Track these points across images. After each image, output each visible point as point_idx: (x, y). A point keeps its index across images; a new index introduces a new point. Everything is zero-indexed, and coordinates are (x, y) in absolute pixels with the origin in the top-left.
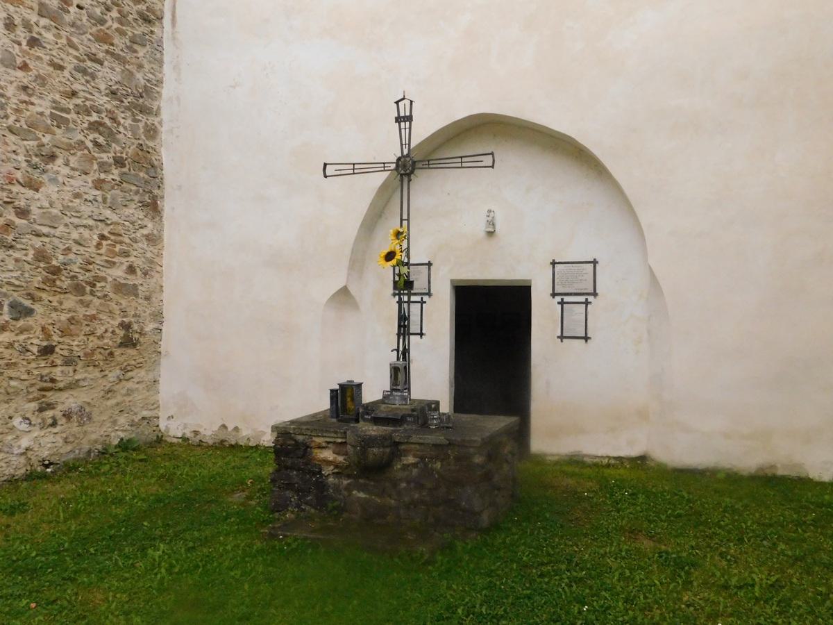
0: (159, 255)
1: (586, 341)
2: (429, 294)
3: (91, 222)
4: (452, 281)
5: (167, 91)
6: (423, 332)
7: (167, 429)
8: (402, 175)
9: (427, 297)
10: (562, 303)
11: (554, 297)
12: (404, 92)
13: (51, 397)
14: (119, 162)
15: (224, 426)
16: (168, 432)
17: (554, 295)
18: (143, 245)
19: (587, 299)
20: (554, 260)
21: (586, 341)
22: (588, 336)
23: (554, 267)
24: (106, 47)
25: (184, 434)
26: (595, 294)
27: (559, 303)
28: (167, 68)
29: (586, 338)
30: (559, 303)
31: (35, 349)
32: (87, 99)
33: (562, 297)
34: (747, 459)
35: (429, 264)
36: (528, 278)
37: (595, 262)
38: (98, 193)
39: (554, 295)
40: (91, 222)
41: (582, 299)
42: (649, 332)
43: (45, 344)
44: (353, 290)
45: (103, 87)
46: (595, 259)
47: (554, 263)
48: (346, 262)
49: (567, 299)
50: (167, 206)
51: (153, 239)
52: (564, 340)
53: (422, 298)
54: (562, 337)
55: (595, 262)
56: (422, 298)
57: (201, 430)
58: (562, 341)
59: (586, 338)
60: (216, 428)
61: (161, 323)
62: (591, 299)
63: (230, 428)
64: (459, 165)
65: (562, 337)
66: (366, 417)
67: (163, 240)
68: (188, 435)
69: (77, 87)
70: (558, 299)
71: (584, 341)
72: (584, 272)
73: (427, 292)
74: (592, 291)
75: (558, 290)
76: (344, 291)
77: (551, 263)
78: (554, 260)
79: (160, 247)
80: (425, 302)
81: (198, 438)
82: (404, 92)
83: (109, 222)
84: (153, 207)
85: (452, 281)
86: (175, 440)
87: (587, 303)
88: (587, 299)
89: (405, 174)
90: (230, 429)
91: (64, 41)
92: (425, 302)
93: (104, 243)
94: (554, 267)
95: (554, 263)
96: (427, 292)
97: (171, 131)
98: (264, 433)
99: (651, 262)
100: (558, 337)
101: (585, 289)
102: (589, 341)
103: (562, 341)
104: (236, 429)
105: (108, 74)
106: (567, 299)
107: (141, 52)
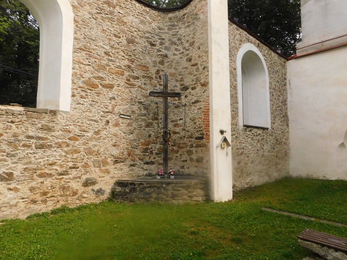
0: (289, 136)
3: (280, 130)
5: (288, 100)
13: (277, 166)
14: (283, 117)
18: (287, 134)
24: (280, 93)
28: (289, 95)
31: (275, 156)
32: (279, 104)
38: (281, 123)
40: (280, 130)
43: (276, 155)
45: (280, 101)
50: (290, 125)
51: (288, 132)
61: (290, 151)
69: (278, 102)
84: (288, 125)
91: (276, 94)
93: (282, 134)
105: (281, 98)
107: (284, 92)
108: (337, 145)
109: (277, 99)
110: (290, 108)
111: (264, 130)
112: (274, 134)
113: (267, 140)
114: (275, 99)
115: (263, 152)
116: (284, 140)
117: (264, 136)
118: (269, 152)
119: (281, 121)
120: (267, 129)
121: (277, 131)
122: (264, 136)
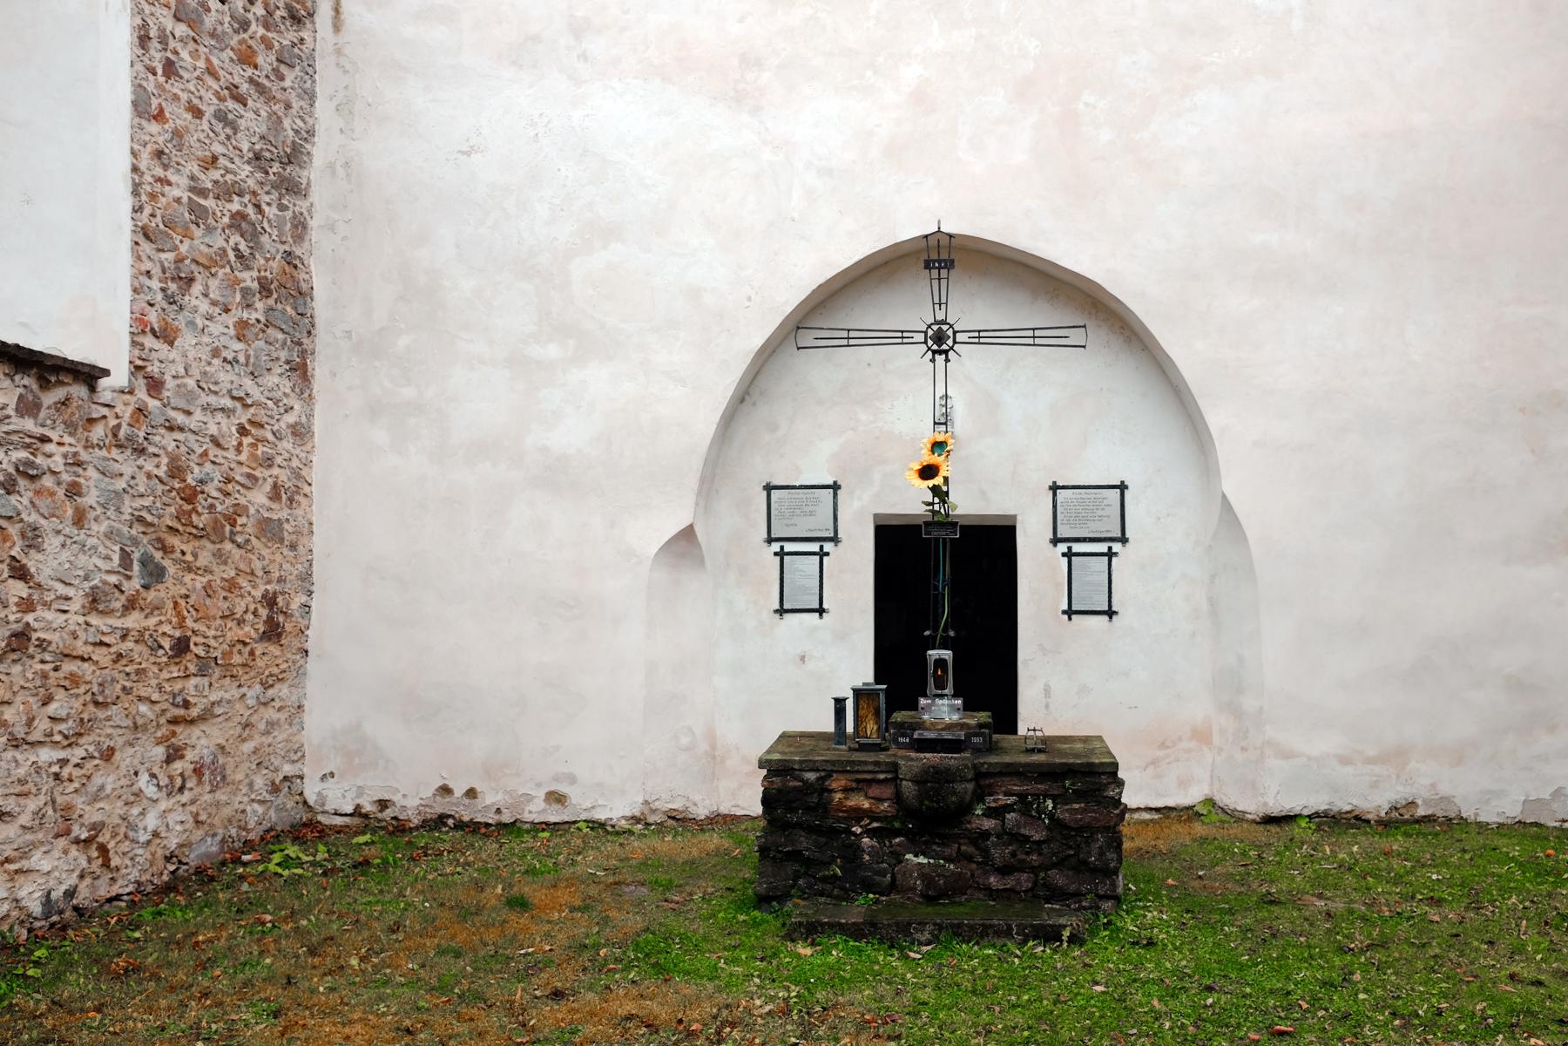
0: (308, 464)
1: (1111, 618)
2: (835, 539)
3: (227, 402)
4: (876, 516)
5: (321, 152)
6: (825, 606)
7: (322, 798)
8: (934, 352)
9: (832, 544)
10: (1069, 555)
11: (1055, 545)
12: (939, 222)
13: (184, 734)
14: (265, 289)
15: (445, 790)
16: (323, 805)
17: (1056, 541)
18: (287, 444)
19: (1110, 548)
20: (1054, 483)
21: (1111, 618)
22: (1114, 609)
23: (1055, 495)
24: (250, 71)
25: (358, 807)
26: (1123, 540)
27: (1064, 555)
28: (324, 110)
29: (1110, 613)
30: (1064, 555)
31: (166, 644)
32: (227, 171)
33: (1069, 544)
34: (1376, 802)
35: (835, 487)
36: (1013, 513)
37: (1122, 487)
38: (239, 346)
39: (1056, 541)
40: (227, 402)
41: (1103, 547)
42: (1212, 602)
43: (177, 634)
44: (698, 530)
45: (245, 146)
46: (1122, 482)
47: (1055, 488)
48: (693, 481)
49: (1077, 548)
50: (320, 370)
51: (301, 432)
52: (1073, 617)
53: (821, 547)
54: (1070, 613)
55: (1122, 487)
56: (821, 547)
57: (396, 798)
58: (1070, 619)
59: (1110, 613)
60: (428, 792)
61: (310, 593)
62: (1116, 547)
63: (459, 791)
64: (1030, 341)
65: (1070, 613)
66: (901, 740)
67: (312, 436)
68: (368, 807)
69: (218, 149)
70: (1063, 547)
71: (1106, 618)
72: (1105, 502)
73: (832, 535)
74: (1119, 535)
75: (1062, 533)
76: (688, 533)
77: (1051, 488)
78: (1054, 483)
79: (308, 447)
80: (827, 554)
81: (388, 813)
82: (939, 222)
83: (249, 401)
84: (300, 371)
85: (876, 516)
86: (339, 821)
87: (1110, 554)
88: (1110, 548)
89: (940, 352)
90: (459, 791)
91: (201, 64)
92: (827, 554)
93: (247, 441)
94: (1055, 495)
95: (1055, 488)
96: (832, 535)
97: (331, 227)
98: (529, 798)
99: (1229, 486)
100: (1064, 612)
101: (1108, 531)
102: (1114, 617)
103: (1070, 619)
104: (471, 793)
105: (252, 121)
106: (1077, 548)
107: (290, 77)
108: (654, 549)
109: (209, 111)
110: (331, 227)
111: (45, 385)
112: (168, 440)
113: (74, 491)
114: (197, 113)
115: (27, 605)
116: (258, 498)
117: (45, 440)
118: (95, 602)
119: (242, 325)
120: (89, 375)
121: (198, 415)
122: (45, 440)
